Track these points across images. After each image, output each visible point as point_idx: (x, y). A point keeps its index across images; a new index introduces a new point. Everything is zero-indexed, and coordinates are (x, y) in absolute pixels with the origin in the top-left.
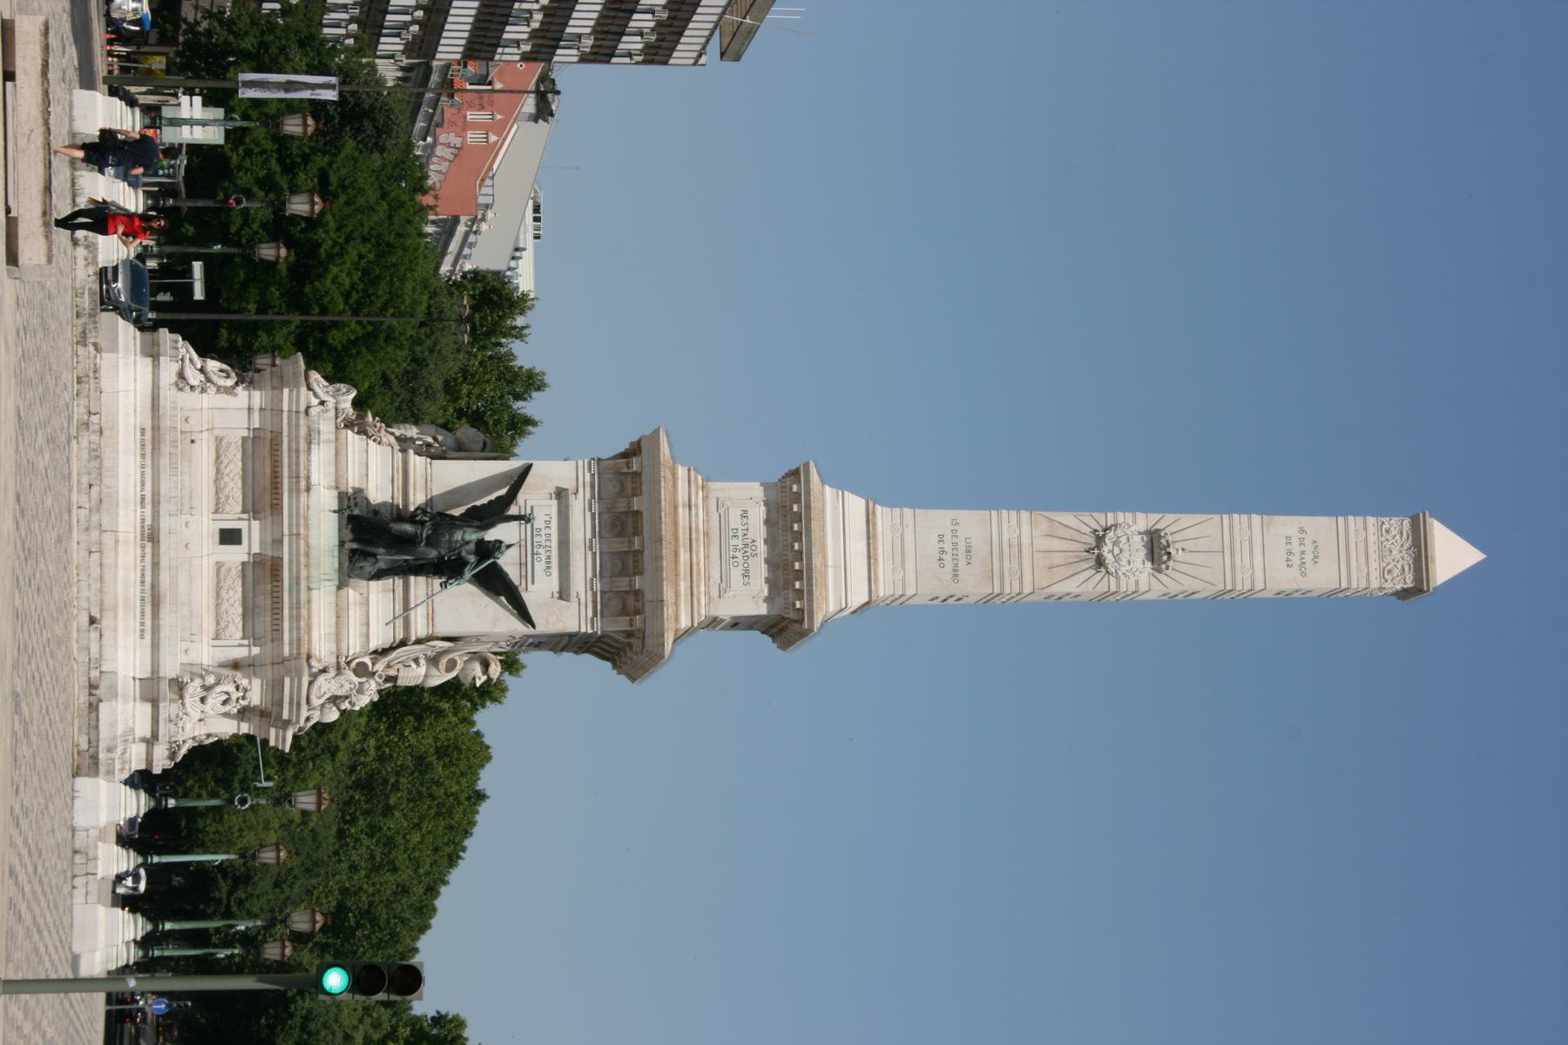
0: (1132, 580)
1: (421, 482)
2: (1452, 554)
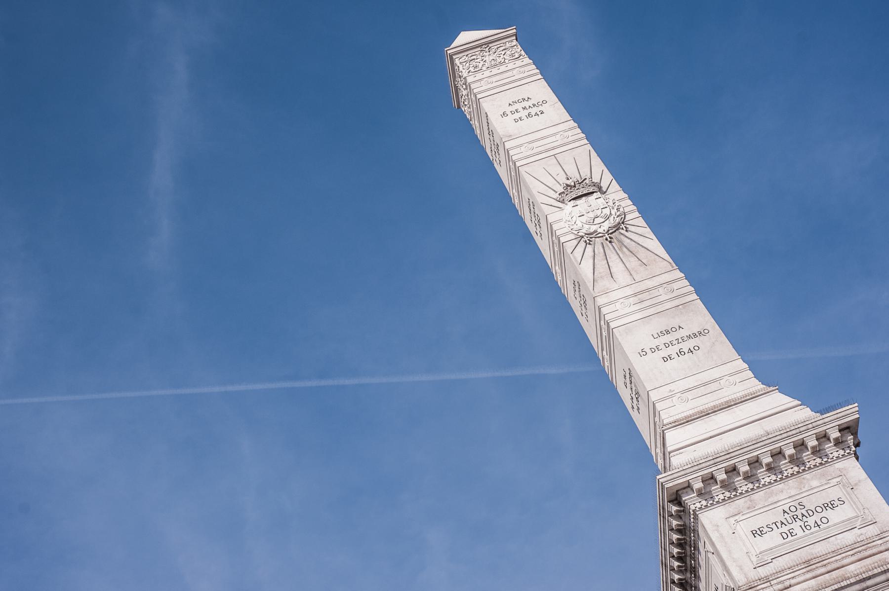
0: (623, 204)
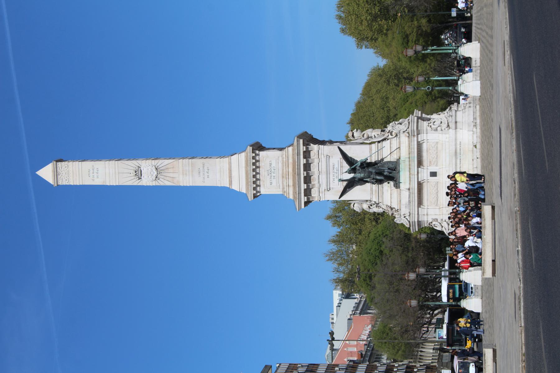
0: (147, 164)
1: (374, 193)
2: (46, 173)
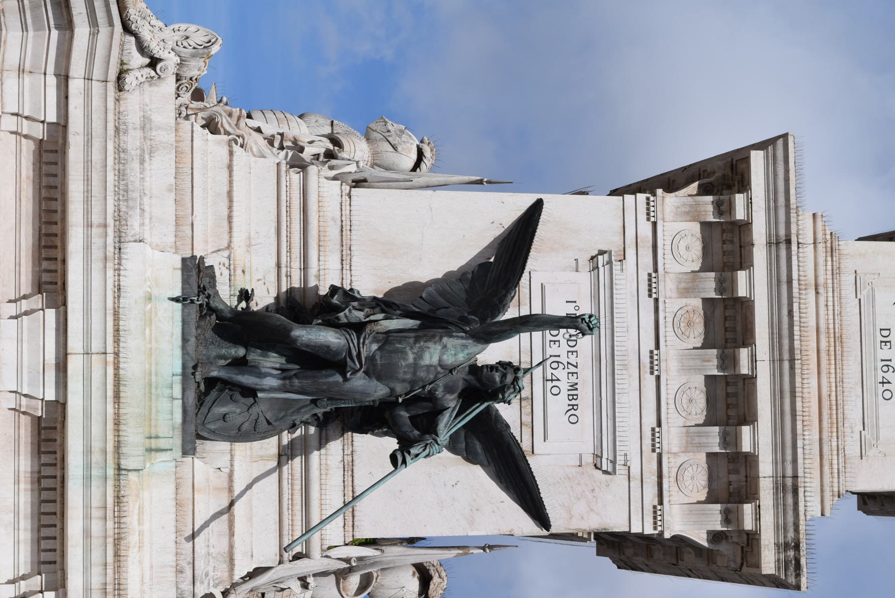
1: (333, 232)
